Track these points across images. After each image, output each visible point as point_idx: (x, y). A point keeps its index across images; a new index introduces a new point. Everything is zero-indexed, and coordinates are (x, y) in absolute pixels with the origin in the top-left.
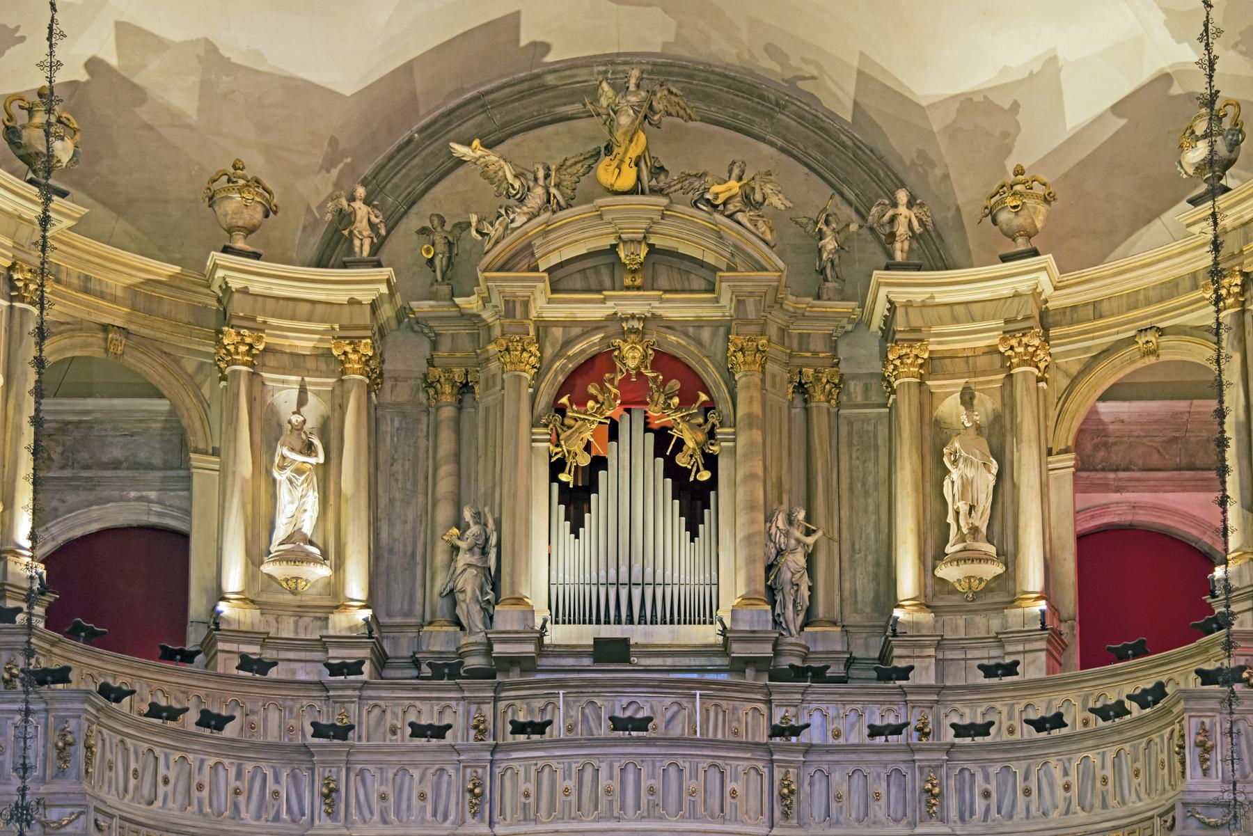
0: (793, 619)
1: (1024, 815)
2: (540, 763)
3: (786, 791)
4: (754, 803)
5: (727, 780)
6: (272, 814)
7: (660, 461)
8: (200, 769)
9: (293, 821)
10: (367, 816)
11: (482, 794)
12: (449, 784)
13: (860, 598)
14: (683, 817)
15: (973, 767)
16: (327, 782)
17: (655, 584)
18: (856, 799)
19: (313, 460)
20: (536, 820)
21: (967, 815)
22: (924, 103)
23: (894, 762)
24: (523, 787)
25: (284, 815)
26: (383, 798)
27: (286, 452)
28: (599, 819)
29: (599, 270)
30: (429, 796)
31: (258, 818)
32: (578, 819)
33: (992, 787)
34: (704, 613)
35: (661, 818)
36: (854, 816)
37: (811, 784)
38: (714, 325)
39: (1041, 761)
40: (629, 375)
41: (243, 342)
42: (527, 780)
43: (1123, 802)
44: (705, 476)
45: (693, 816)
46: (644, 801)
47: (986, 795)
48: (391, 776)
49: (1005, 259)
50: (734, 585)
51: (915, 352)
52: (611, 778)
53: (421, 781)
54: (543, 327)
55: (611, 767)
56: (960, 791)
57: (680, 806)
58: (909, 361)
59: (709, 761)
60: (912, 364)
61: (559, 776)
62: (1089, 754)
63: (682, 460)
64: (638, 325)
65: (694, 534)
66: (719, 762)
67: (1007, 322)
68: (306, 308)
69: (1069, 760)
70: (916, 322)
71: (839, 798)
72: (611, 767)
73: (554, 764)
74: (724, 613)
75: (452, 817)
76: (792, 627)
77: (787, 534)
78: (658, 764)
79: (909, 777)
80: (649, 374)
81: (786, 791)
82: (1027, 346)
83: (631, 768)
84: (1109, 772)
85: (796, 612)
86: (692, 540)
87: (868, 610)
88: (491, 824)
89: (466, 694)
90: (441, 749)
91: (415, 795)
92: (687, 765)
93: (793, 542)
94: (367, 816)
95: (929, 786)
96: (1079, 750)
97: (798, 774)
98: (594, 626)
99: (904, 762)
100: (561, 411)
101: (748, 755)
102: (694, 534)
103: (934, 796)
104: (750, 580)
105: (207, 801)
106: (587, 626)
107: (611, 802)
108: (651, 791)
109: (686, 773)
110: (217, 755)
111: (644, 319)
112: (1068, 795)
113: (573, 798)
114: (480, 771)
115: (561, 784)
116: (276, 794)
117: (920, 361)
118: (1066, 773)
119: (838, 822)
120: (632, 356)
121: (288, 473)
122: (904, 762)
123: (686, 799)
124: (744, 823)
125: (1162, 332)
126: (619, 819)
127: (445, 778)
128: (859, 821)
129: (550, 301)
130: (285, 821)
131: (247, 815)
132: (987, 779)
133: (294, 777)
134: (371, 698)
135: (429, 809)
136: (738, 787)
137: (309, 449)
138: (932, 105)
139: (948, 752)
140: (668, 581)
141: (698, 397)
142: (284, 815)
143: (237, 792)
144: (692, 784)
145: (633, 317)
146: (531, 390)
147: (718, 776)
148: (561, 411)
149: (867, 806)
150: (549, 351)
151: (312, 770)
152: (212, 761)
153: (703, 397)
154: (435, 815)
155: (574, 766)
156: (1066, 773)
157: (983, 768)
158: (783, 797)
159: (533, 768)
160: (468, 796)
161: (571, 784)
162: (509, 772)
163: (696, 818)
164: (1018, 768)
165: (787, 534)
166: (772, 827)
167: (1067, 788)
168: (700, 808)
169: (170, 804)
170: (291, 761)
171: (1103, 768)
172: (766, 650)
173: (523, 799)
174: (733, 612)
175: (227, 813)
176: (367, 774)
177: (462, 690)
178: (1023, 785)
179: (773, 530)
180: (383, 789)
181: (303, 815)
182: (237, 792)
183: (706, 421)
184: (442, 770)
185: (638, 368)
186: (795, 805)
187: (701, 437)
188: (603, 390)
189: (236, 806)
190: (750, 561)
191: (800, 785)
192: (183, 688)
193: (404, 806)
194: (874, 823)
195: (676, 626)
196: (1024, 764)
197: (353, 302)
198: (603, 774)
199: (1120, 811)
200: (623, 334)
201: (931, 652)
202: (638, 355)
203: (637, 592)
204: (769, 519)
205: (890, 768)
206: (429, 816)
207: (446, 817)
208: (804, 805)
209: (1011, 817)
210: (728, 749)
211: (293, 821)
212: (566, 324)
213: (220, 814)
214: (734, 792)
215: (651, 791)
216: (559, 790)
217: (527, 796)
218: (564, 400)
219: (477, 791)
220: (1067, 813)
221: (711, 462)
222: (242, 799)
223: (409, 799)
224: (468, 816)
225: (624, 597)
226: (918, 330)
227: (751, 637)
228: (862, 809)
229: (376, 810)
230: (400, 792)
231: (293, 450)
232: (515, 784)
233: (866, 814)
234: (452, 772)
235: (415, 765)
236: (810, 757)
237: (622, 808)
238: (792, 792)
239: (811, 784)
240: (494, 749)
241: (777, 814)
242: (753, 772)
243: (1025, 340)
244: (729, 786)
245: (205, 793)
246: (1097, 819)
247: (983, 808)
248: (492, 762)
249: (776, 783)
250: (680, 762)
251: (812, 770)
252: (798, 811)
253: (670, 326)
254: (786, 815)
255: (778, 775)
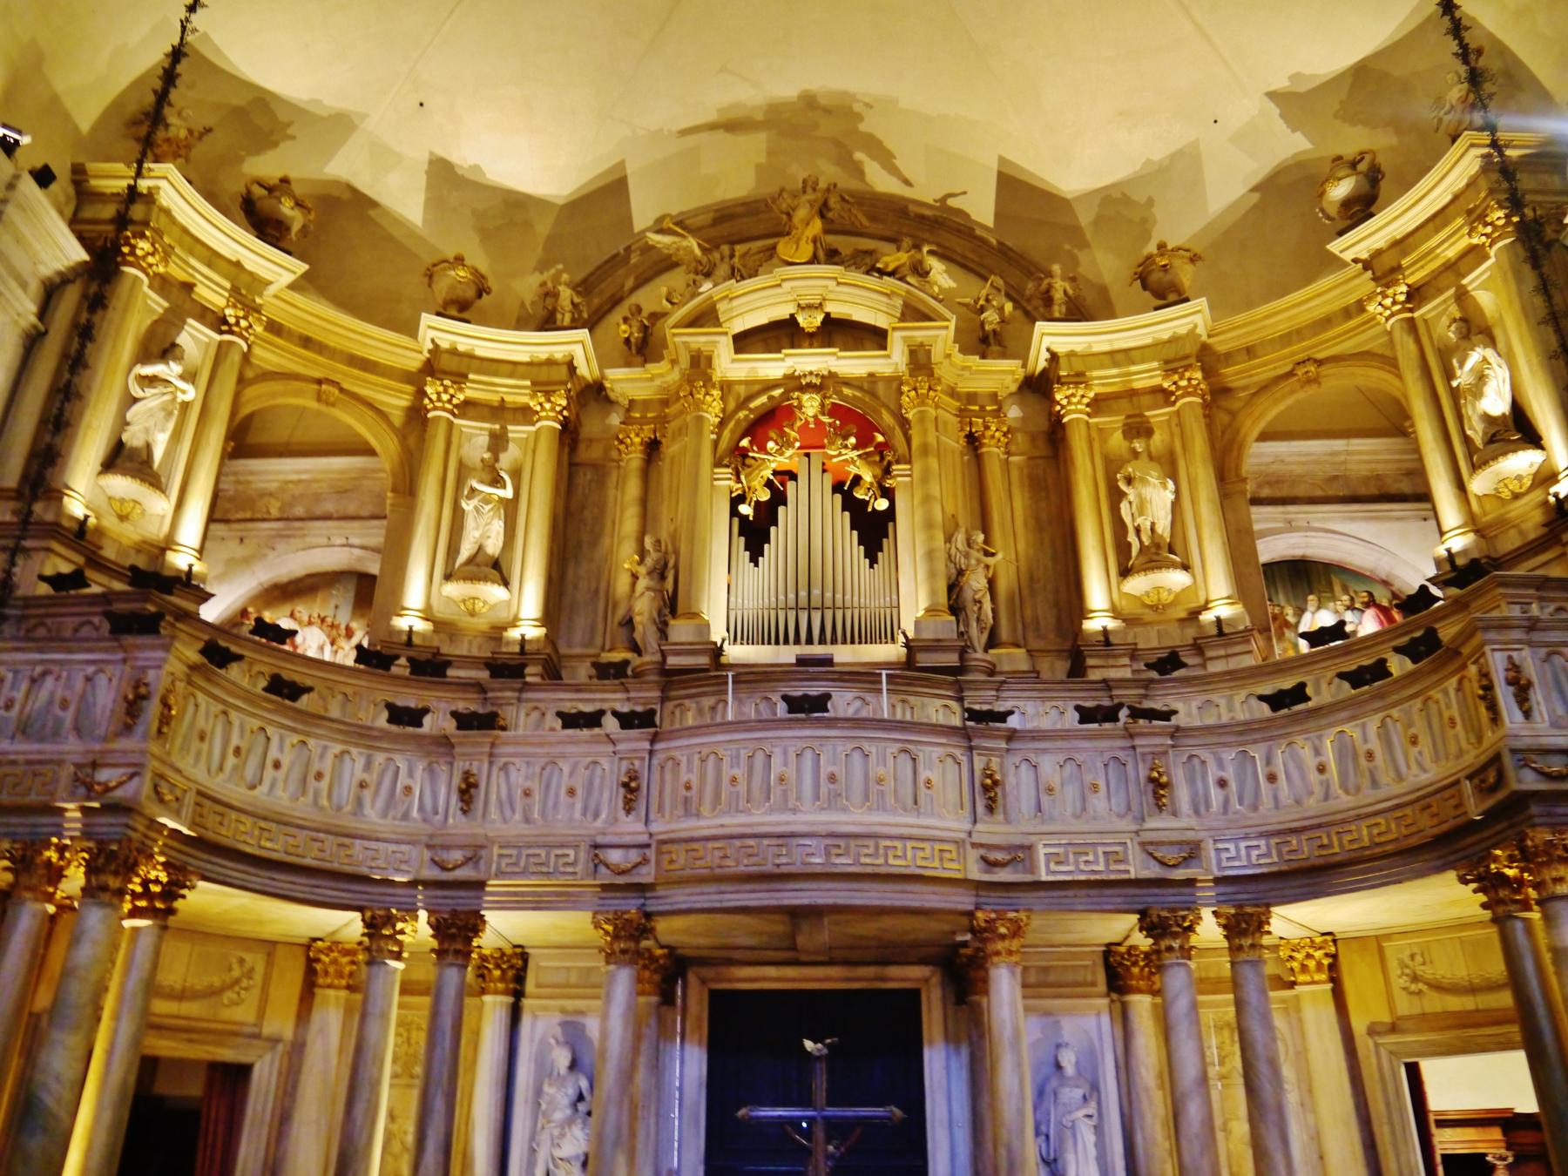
0: (978, 638)
1: (1271, 805)
2: (705, 751)
3: (989, 781)
4: (952, 796)
5: (921, 768)
6: (401, 810)
7: (838, 497)
8: (322, 757)
9: (425, 820)
10: (508, 813)
11: (637, 789)
12: (603, 778)
13: (1042, 624)
14: (870, 809)
15: (1204, 754)
16: (467, 775)
17: (834, 608)
18: (1071, 793)
19: (501, 493)
20: (698, 815)
21: (1202, 809)
22: (1069, 196)
23: (1111, 749)
24: (684, 777)
25: (415, 813)
26: (527, 793)
27: (476, 485)
28: (771, 811)
29: (782, 334)
30: (580, 792)
31: (384, 815)
32: (748, 812)
33: (1230, 774)
34: (886, 634)
35: (845, 810)
36: (1069, 809)
37: (1016, 774)
38: (889, 380)
39: (1284, 742)
40: (807, 422)
41: (446, 391)
42: (690, 770)
43: (1400, 778)
44: (882, 504)
45: (882, 807)
46: (824, 789)
47: (1222, 783)
48: (538, 769)
49: (1156, 309)
50: (914, 601)
51: (1080, 392)
52: (786, 764)
53: (571, 775)
54: (726, 387)
55: (785, 753)
56: (1191, 781)
57: (867, 798)
58: (1074, 400)
59: (899, 745)
60: (1079, 403)
61: (725, 765)
62: (1346, 728)
63: (859, 494)
64: (817, 381)
65: (873, 561)
66: (911, 747)
67: (1167, 362)
68: (508, 368)
69: (1320, 737)
70: (1078, 366)
71: (1050, 790)
72: (785, 753)
73: (721, 752)
74: (908, 626)
75: (603, 816)
76: (976, 644)
77: (967, 556)
78: (840, 749)
79: (1130, 767)
80: (826, 419)
81: (989, 781)
82: (1189, 379)
83: (808, 754)
84: (1375, 744)
85: (982, 630)
86: (871, 566)
87: (1052, 636)
88: (647, 822)
89: (632, 695)
90: (595, 741)
91: (563, 791)
92: (873, 750)
93: (973, 562)
94: (508, 813)
95: (1155, 774)
96: (1331, 725)
97: (1002, 765)
98: (772, 648)
99: (1123, 749)
100: (744, 454)
101: (944, 741)
102: (873, 561)
103: (1163, 786)
104: (933, 593)
105: (324, 793)
106: (766, 647)
107: (785, 793)
108: (832, 778)
109: (873, 759)
110: (343, 742)
111: (823, 377)
112: (1323, 777)
113: (742, 787)
114: (637, 763)
115: (727, 772)
116: (408, 790)
117: (1086, 401)
118: (1317, 752)
119: (1051, 818)
120: (810, 405)
121: (475, 502)
122: (1123, 749)
123: (874, 787)
124: (941, 817)
125: (1320, 363)
126: (795, 811)
127: (599, 771)
128: (1076, 817)
129: (734, 361)
130: (415, 820)
131: (372, 813)
132: (1221, 765)
133: (430, 770)
134: (530, 700)
135: (579, 806)
136: (934, 776)
137: (497, 481)
138: (1078, 198)
139: (1172, 737)
140: (848, 604)
141: (873, 438)
142: (415, 813)
143: (362, 785)
144: (881, 771)
145: (811, 373)
146: (714, 436)
147: (909, 764)
148: (744, 454)
149: (1084, 800)
150: (732, 405)
151: (451, 764)
152: (337, 748)
153: (880, 438)
154: (584, 814)
155: (743, 752)
156: (1317, 752)
157: (1214, 754)
158: (986, 789)
159: (697, 757)
160: (622, 791)
161: (739, 772)
162: (670, 764)
163: (884, 810)
164: (1257, 752)
165: (967, 556)
166: (975, 822)
167: (1322, 769)
168: (890, 799)
169: (279, 792)
170: (428, 754)
171: (1365, 740)
172: (951, 659)
173: (684, 793)
174: (917, 623)
175: (349, 808)
176: (512, 769)
177: (627, 691)
178: (1267, 770)
179: (953, 551)
180: (528, 784)
181: (436, 813)
182: (362, 785)
183: (882, 459)
184: (595, 763)
185: (815, 417)
186: (1000, 799)
187: (879, 472)
188: (783, 434)
189: (359, 802)
190: (932, 575)
191: (1003, 775)
192: (330, 684)
193: (550, 803)
194: (1094, 818)
195: (857, 646)
196: (1263, 747)
197: (550, 362)
198: (776, 762)
199: (1397, 789)
200: (804, 389)
201: (1126, 661)
202: (816, 404)
203: (816, 618)
204: (949, 539)
205: (1107, 755)
206: (577, 815)
207: (596, 815)
208: (1010, 799)
209: (1255, 808)
210: (920, 732)
211: (425, 820)
212: (747, 383)
213: (339, 809)
214: (928, 782)
215: (832, 778)
216: (725, 780)
217: (688, 787)
218: (745, 443)
219: (633, 784)
220: (1326, 797)
221: (888, 493)
222: (367, 794)
223: (557, 795)
224: (622, 813)
225: (809, 617)
226: (1080, 374)
227: (936, 646)
228: (1078, 804)
229: (519, 808)
230: (548, 787)
231: (482, 482)
232: (676, 777)
233: (1084, 809)
234: (606, 766)
235: (563, 756)
236: (1015, 745)
237: (799, 798)
238: (996, 783)
239: (1016, 774)
240: (654, 739)
241: (980, 809)
242: (950, 760)
243: (1187, 375)
244: (924, 774)
245: (325, 784)
246: (1367, 801)
247: (1221, 798)
248: (651, 753)
249: (978, 773)
250: (866, 746)
251: (1017, 759)
252: (1004, 806)
253: (847, 382)
254: (990, 809)
255: (979, 763)
